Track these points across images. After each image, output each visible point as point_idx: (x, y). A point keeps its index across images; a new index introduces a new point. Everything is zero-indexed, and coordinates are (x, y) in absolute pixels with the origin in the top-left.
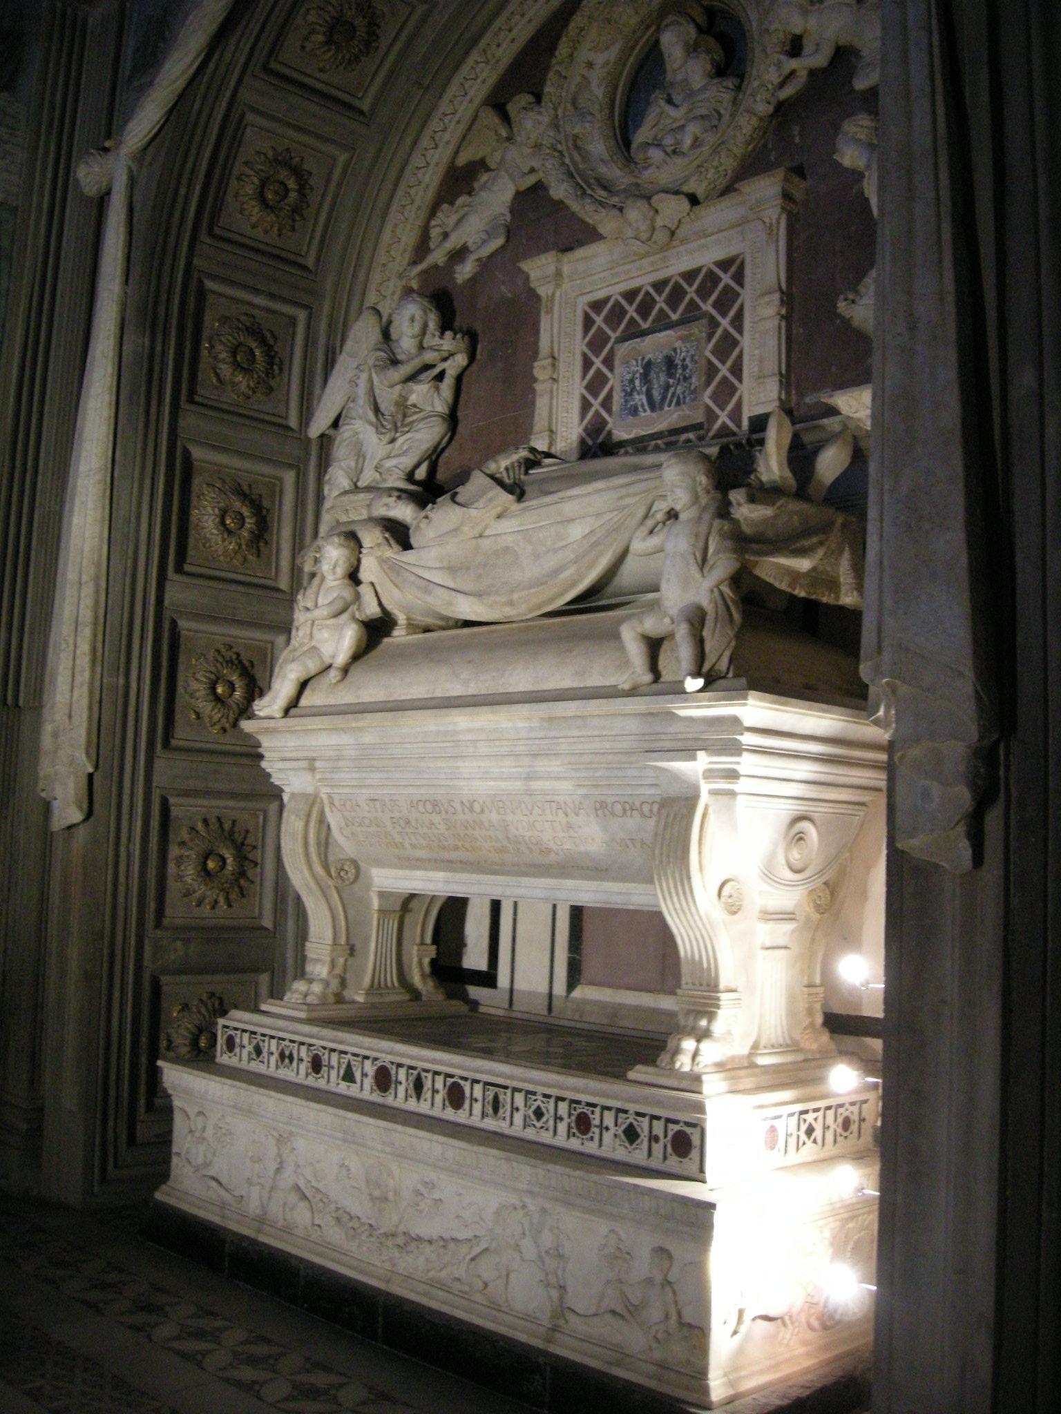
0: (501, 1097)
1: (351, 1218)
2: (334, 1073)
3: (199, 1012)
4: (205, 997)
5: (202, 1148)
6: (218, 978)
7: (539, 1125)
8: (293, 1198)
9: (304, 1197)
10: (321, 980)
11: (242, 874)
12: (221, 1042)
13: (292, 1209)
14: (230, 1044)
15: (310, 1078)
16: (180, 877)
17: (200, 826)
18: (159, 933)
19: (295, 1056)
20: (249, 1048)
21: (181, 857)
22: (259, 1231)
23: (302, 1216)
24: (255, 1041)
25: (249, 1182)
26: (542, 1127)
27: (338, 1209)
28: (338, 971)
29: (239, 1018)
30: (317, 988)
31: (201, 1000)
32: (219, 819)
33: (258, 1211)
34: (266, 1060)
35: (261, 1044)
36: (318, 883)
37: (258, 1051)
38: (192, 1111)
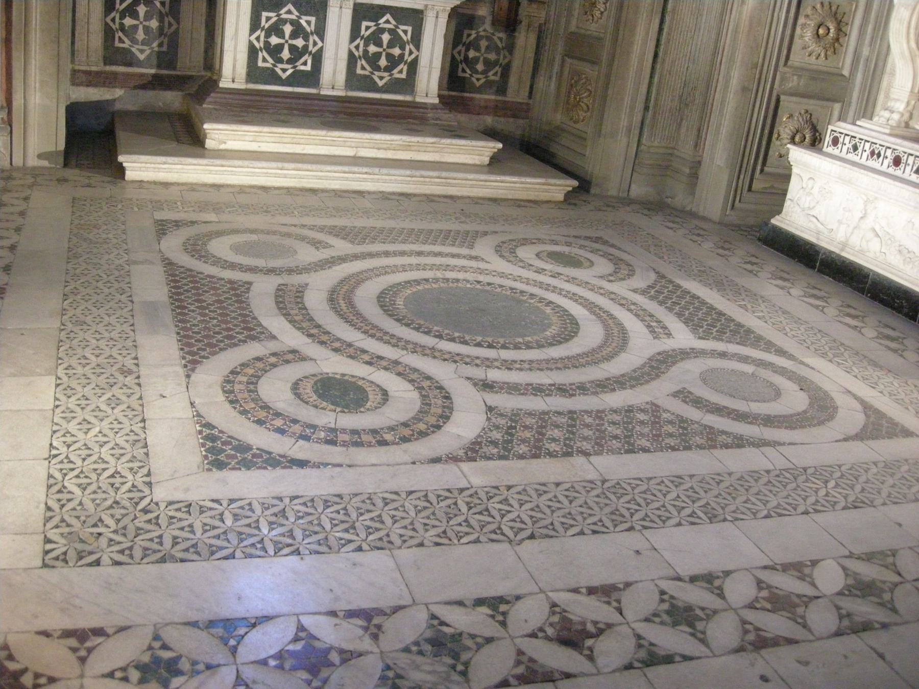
1: (909, 252)
2: (908, 169)
3: (798, 120)
4: (803, 112)
5: (809, 199)
6: (812, 101)
8: (870, 235)
9: (877, 235)
10: (899, 112)
11: (837, 40)
12: (828, 139)
13: (867, 242)
14: (835, 142)
15: (890, 168)
16: (802, 37)
17: (818, 6)
18: (786, 69)
20: (850, 145)
21: (805, 24)
22: (842, 250)
23: (874, 246)
24: (854, 142)
25: (840, 222)
27: (900, 246)
28: (910, 108)
29: (843, 127)
30: (896, 116)
31: (800, 114)
32: (830, 3)
33: (843, 239)
34: (860, 154)
35: (858, 144)
36: (910, 52)
37: (855, 148)
38: (805, 177)
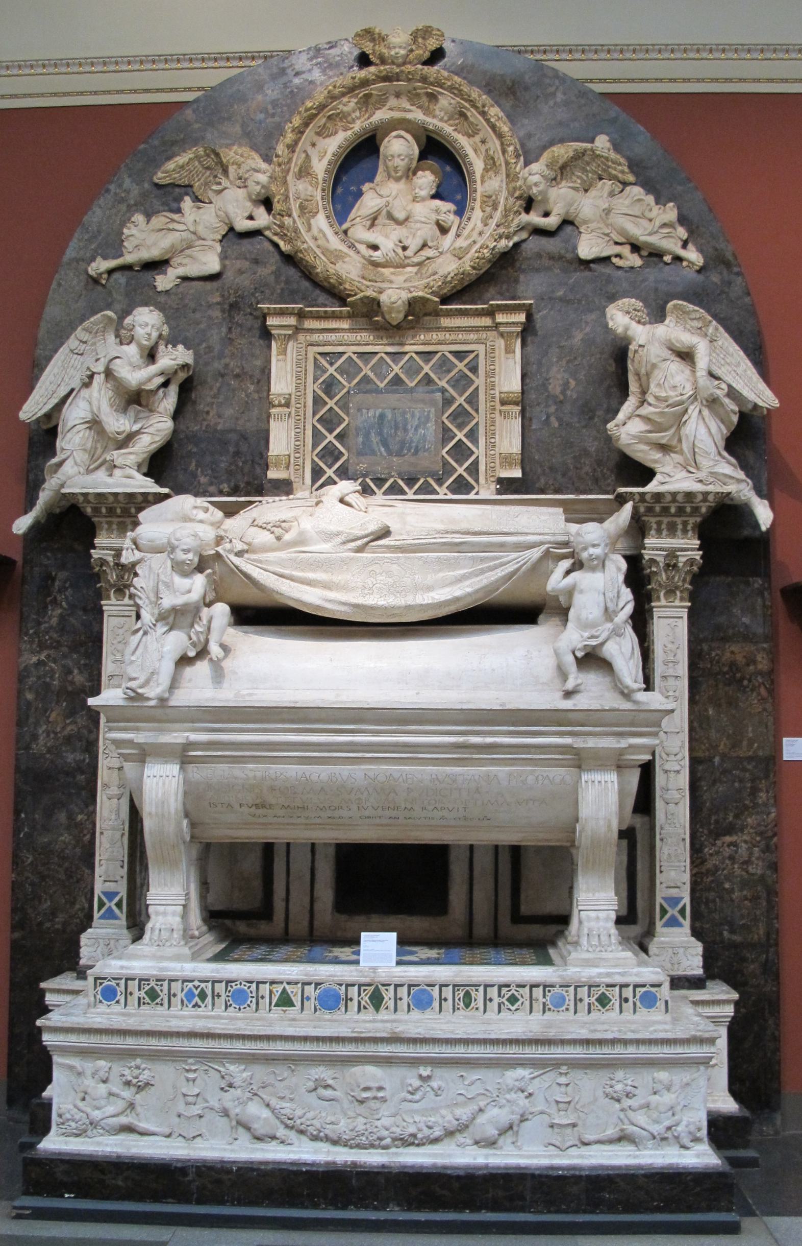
0: (473, 994)
7: (513, 1008)
19: (209, 992)
20: (142, 994)
26: (517, 1010)
37: (153, 995)
